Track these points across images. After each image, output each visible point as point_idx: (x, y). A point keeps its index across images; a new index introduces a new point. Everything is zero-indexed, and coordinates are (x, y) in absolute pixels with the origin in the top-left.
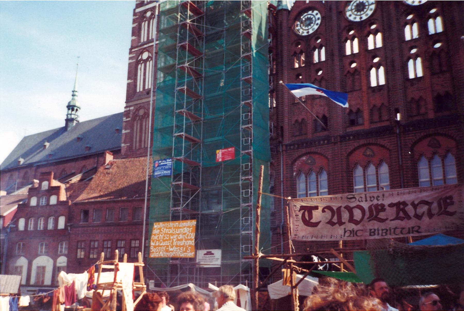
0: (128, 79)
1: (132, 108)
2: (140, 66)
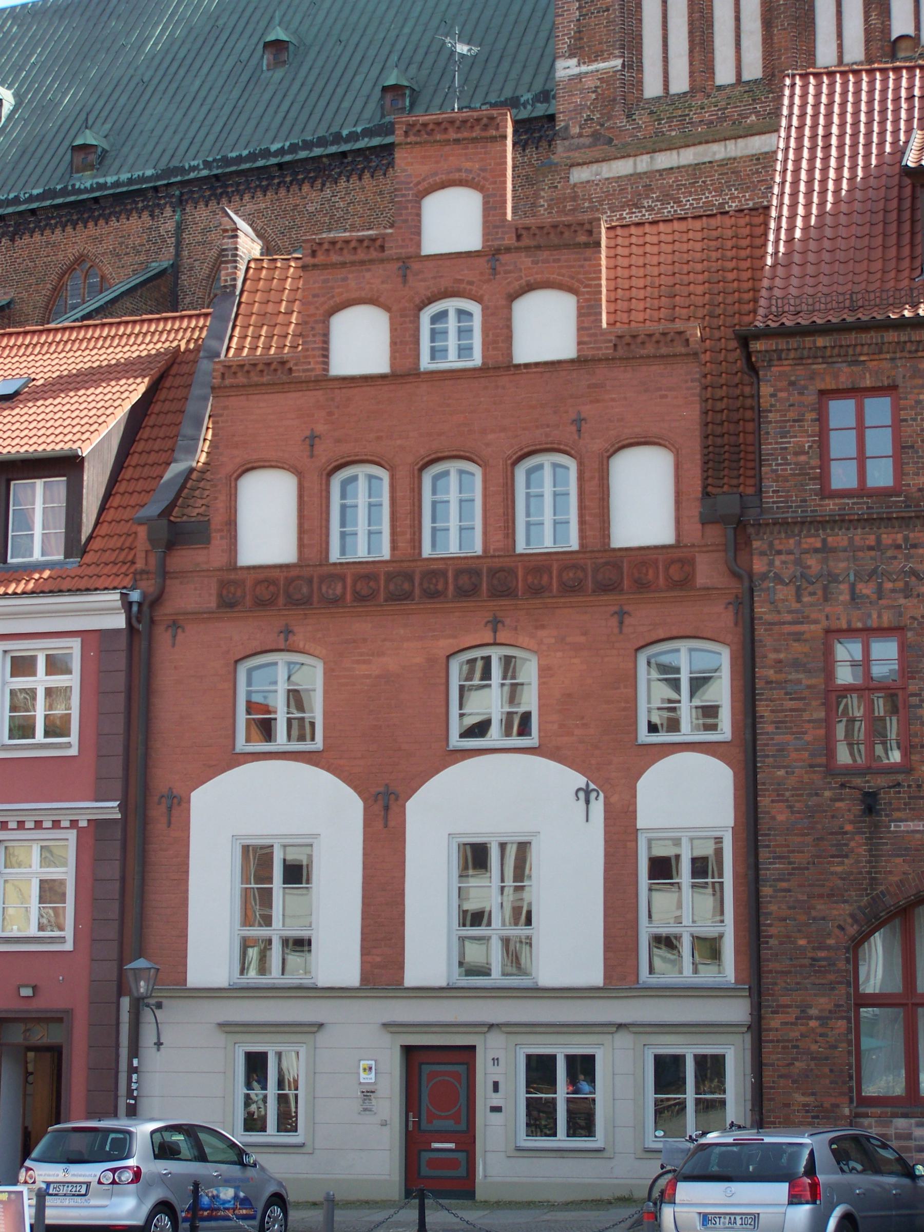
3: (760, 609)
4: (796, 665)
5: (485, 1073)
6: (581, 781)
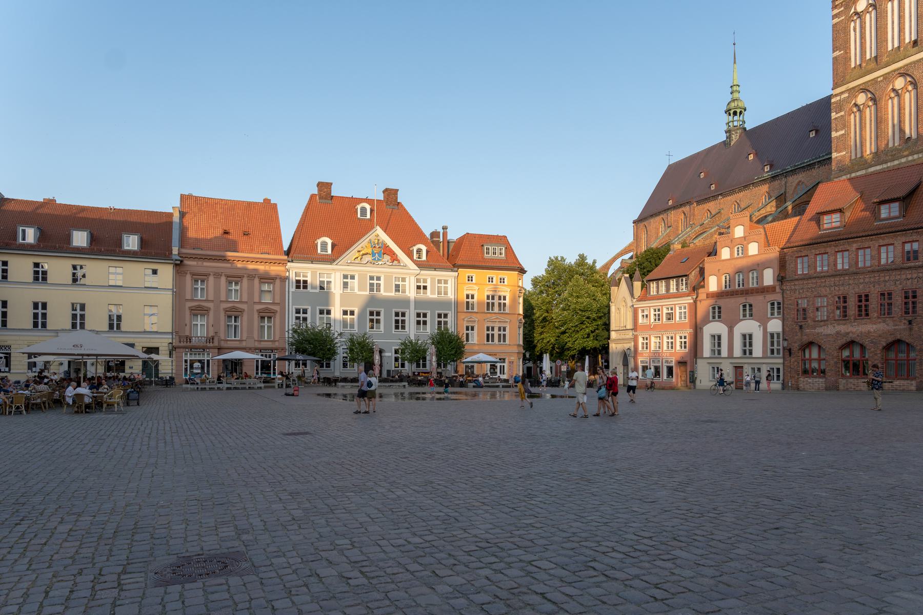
0: (834, 51)
1: (846, 95)
2: (852, 24)
3: (785, 295)
4: (790, 304)
5: (745, 370)
6: (759, 324)
